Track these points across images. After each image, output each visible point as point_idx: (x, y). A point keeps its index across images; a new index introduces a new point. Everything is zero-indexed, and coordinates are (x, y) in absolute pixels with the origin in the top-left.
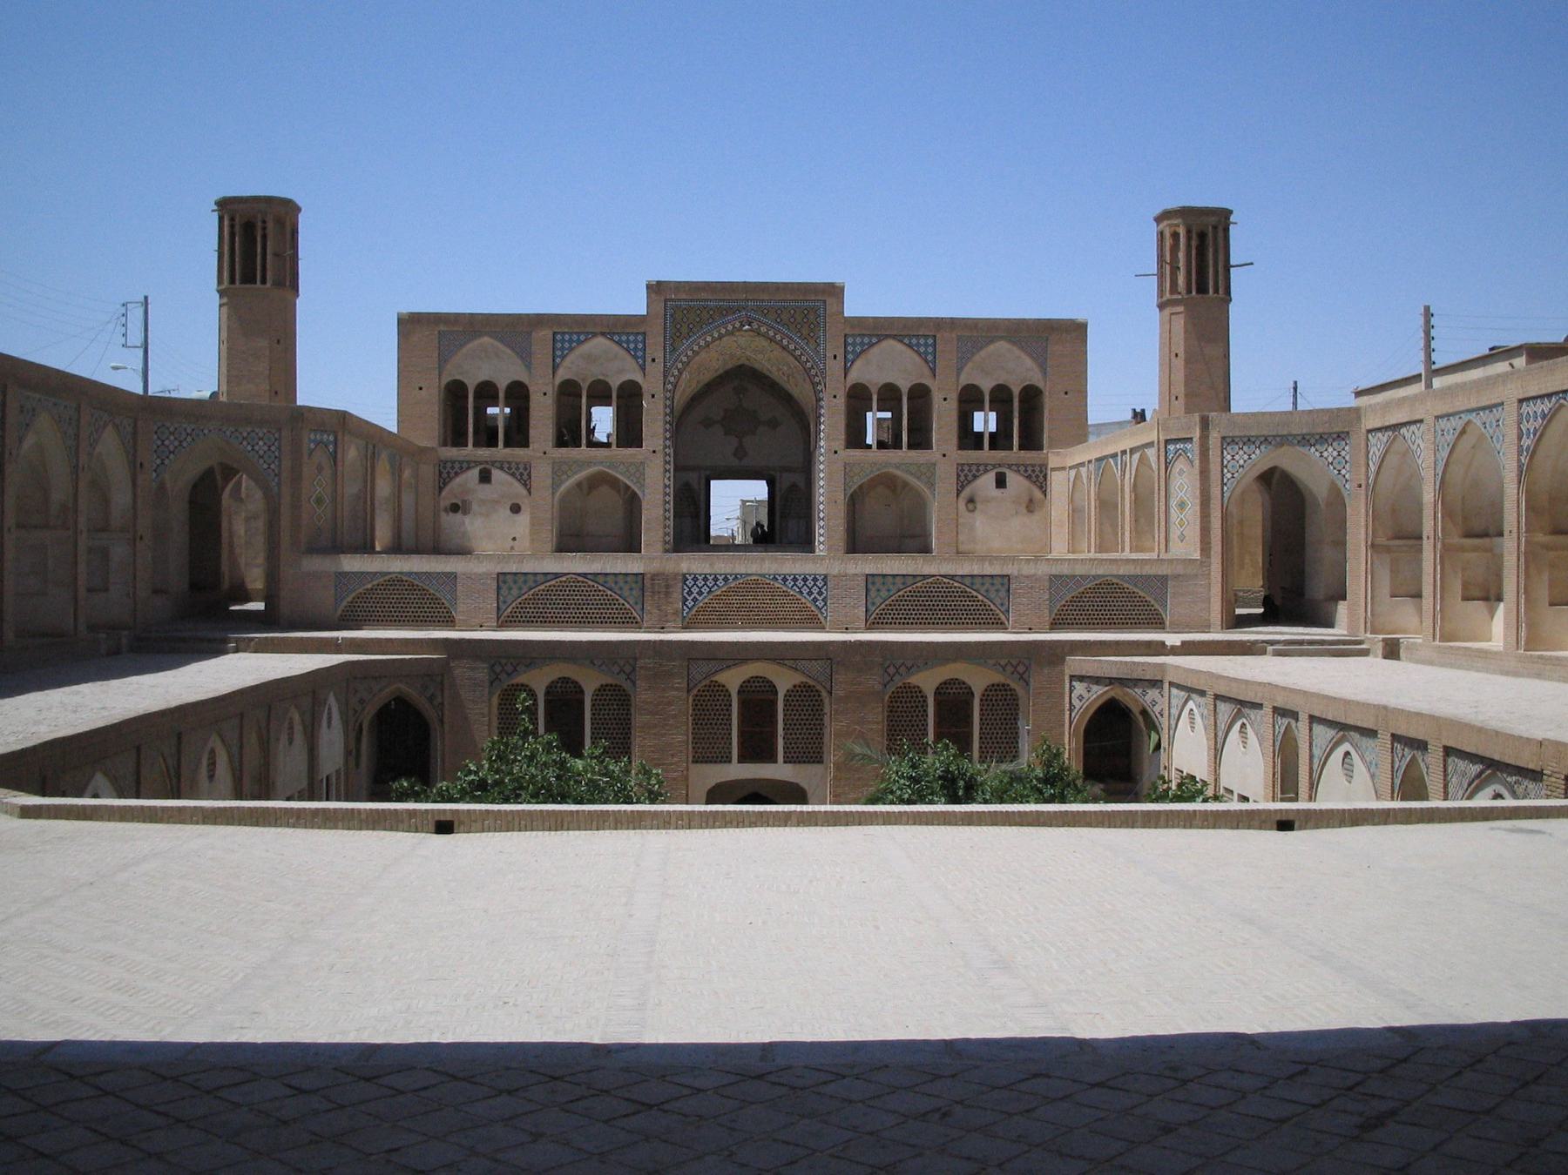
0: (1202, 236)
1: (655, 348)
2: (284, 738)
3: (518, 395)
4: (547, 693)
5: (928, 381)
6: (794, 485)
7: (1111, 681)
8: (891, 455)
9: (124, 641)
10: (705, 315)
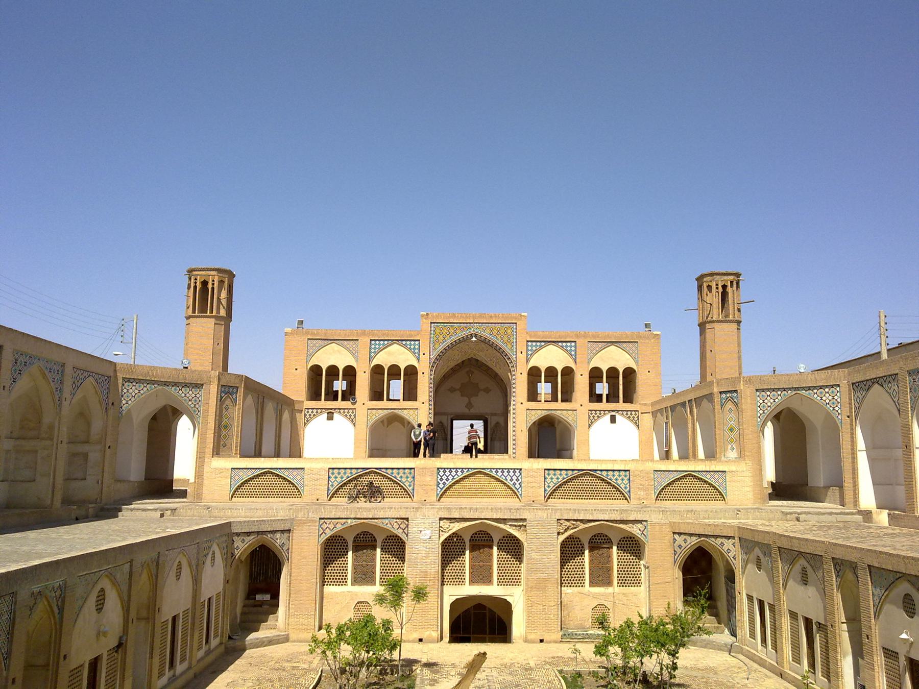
0: (724, 287)
1: (425, 348)
2: (173, 574)
3: (350, 373)
4: (354, 541)
5: (573, 366)
6: (498, 423)
7: (700, 536)
8: (553, 405)
9: (91, 511)
10: (452, 331)
